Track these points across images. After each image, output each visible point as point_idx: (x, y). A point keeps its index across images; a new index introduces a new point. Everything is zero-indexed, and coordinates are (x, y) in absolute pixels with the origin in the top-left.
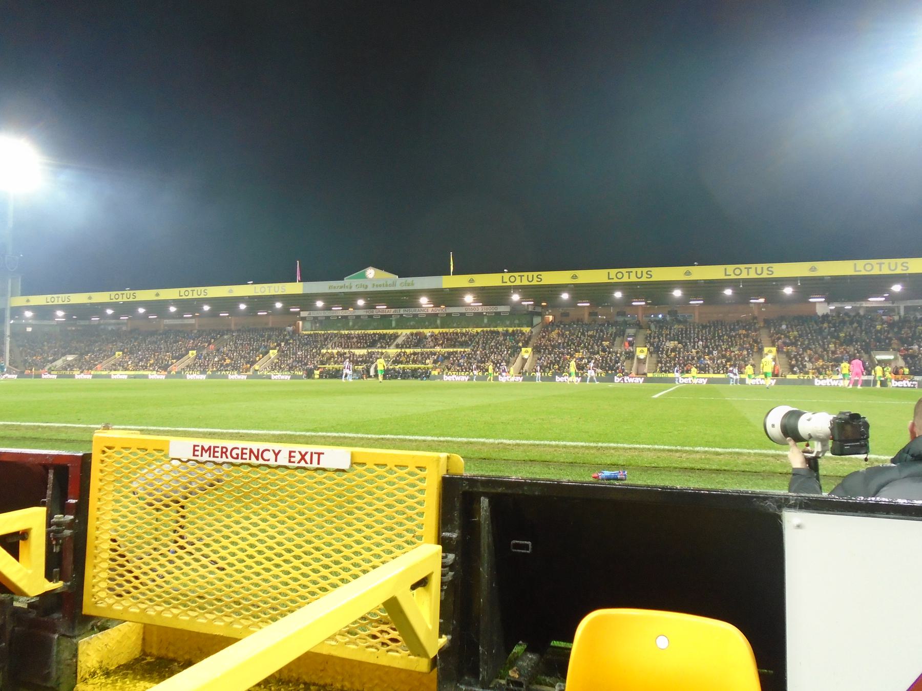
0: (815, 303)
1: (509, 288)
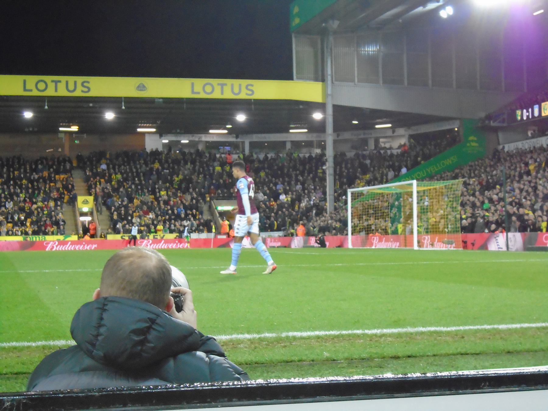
0: (143, 134)
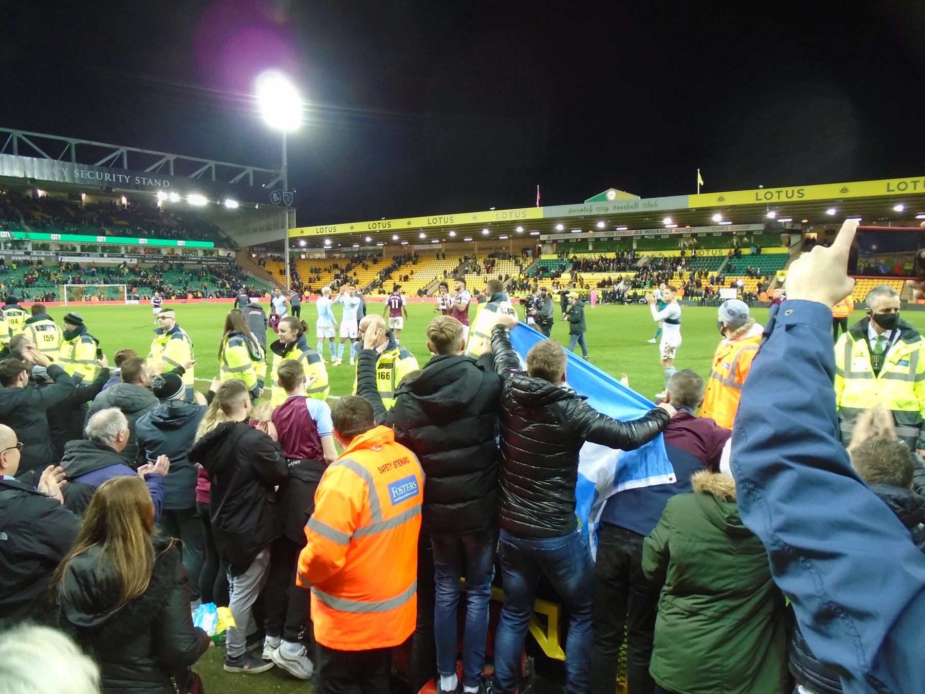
1: (765, 205)
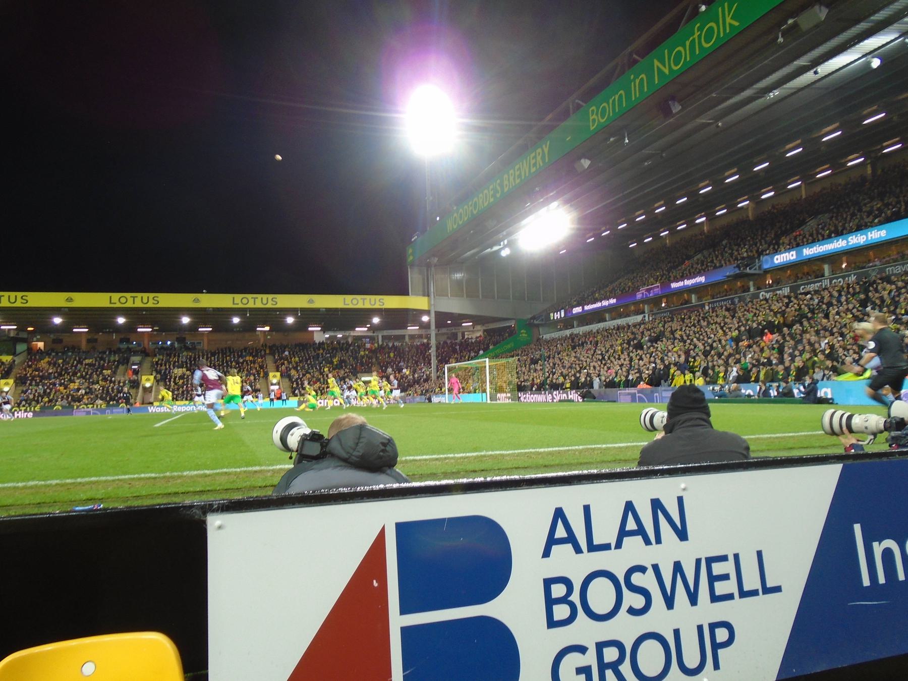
0: (313, 332)
